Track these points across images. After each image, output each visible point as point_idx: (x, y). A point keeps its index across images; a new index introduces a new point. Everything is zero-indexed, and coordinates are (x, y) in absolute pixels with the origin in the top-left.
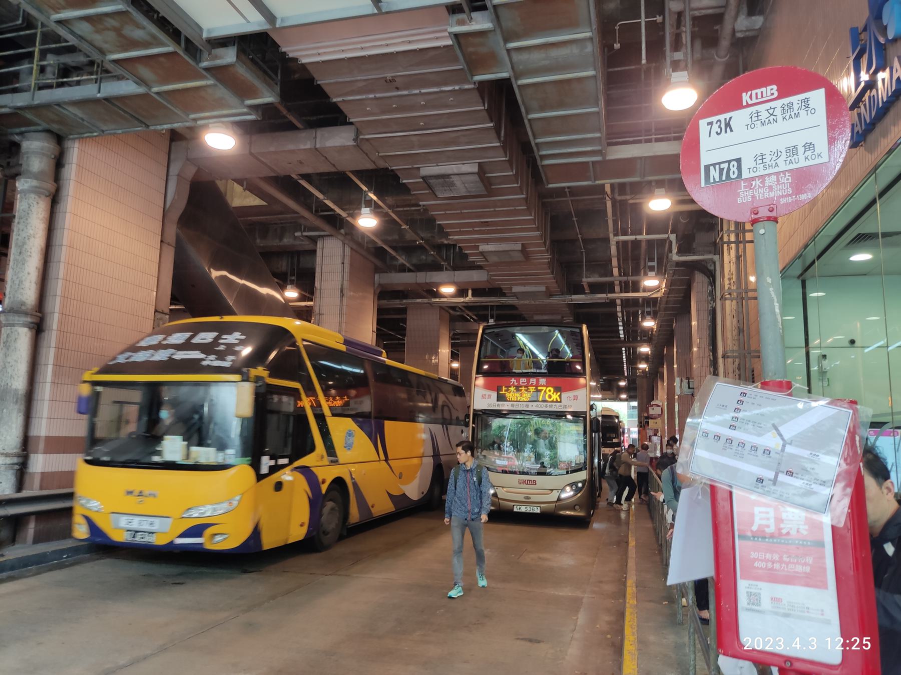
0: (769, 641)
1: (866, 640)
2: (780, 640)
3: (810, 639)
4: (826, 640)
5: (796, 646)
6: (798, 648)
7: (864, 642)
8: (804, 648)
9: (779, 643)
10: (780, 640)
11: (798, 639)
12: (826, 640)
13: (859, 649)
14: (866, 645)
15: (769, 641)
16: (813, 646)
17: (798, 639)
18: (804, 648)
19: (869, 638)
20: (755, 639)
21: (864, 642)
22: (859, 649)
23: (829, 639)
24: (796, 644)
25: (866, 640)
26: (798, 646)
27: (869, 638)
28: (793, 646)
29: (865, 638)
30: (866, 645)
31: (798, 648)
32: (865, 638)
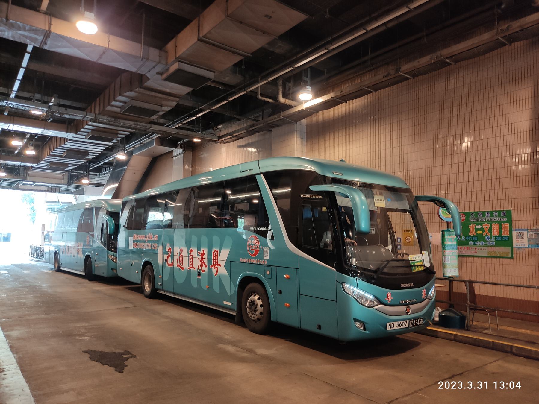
0: (454, 383)
2: (460, 383)
4: (494, 383)
5: (518, 387)
6: (519, 388)
8: (465, 388)
10: (480, 383)
11: (519, 383)
12: (494, 383)
13: (443, 388)
15: (454, 383)
16: (502, 387)
17: (519, 383)
18: (475, 388)
22: (443, 388)
23: (496, 383)
24: (518, 385)
26: (519, 387)
28: (516, 386)
31: (519, 388)
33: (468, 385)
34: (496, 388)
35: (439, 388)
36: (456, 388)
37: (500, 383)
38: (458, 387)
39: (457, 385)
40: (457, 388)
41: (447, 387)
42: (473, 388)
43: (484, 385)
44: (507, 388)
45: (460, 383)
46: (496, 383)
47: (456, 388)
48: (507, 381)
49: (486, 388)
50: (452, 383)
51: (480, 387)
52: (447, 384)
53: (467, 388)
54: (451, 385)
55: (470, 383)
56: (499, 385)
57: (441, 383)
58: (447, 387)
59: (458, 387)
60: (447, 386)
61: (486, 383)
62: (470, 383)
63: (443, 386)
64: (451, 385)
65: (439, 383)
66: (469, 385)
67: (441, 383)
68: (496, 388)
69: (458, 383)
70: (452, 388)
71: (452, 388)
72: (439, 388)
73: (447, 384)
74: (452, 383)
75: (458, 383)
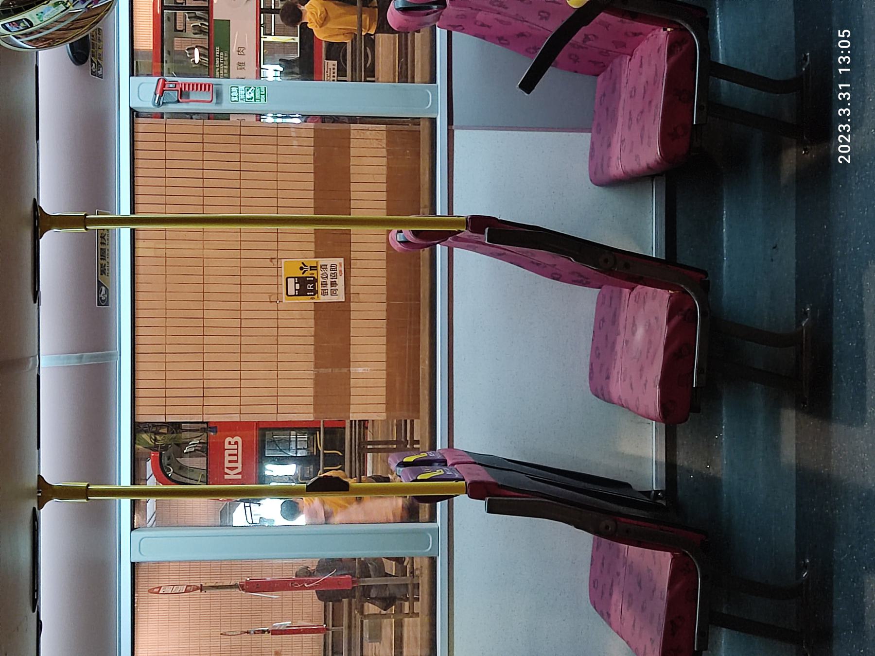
0: (842, 139)
1: (841, 34)
2: (842, 128)
3: (840, 115)
4: (841, 73)
7: (843, 36)
9: (844, 129)
10: (841, 96)
12: (841, 73)
14: (846, 34)
15: (842, 139)
16: (847, 60)
18: (849, 104)
19: (839, 31)
20: (840, 152)
21: (843, 36)
23: (840, 70)
25: (841, 34)
27: (839, 31)
29: (840, 35)
30: (846, 34)
32: (840, 35)
33: (844, 116)
34: (849, 70)
35: (849, 162)
36: (849, 135)
37: (840, 63)
38: (848, 131)
39: (845, 133)
40: (849, 133)
41: (847, 149)
42: (848, 107)
43: (844, 90)
44: (849, 52)
45: (842, 128)
46: (840, 70)
47: (849, 135)
48: (838, 52)
50: (841, 141)
51: (847, 96)
52: (842, 149)
53: (849, 117)
54: (845, 142)
55: (842, 112)
56: (844, 65)
57: (842, 159)
58: (847, 149)
59: (848, 131)
60: (846, 149)
61: (840, 86)
62: (842, 112)
63: (846, 155)
64: (845, 142)
65: (841, 162)
66: (844, 113)
67: (842, 159)
68: (849, 70)
69: (840, 131)
70: (849, 141)
71: (849, 141)
72: (849, 162)
73: (842, 149)
74: (841, 141)
75: (840, 131)
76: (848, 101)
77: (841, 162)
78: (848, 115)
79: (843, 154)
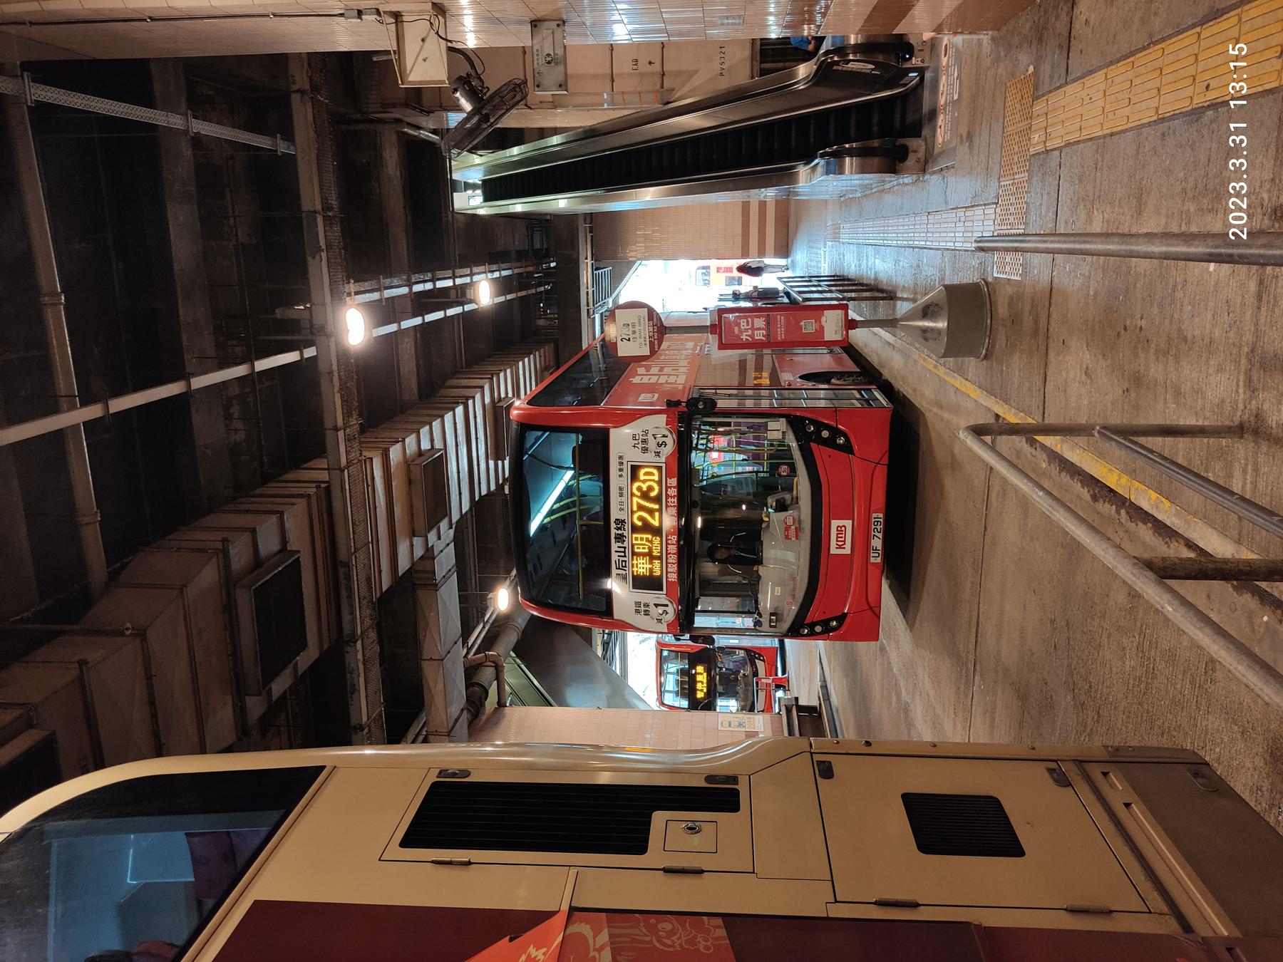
1: (1233, 49)
10: (1234, 141)
13: (1245, 229)
14: (1241, 50)
19: (1231, 46)
25: (1233, 49)
27: (1231, 46)
29: (1231, 52)
30: (1241, 50)
32: (1231, 52)
33: (1237, 170)
35: (1245, 237)
36: (1245, 198)
38: (1244, 192)
39: (1238, 195)
40: (1244, 195)
41: (1242, 218)
43: (1238, 132)
45: (1234, 188)
46: (1232, 103)
47: (1245, 198)
49: (1245, 125)
50: (1233, 207)
51: (1242, 141)
52: (1235, 218)
53: (1245, 171)
54: (1240, 209)
55: (1234, 165)
57: (1234, 234)
58: (1242, 218)
59: (1244, 192)
60: (1241, 218)
61: (1232, 126)
62: (1234, 165)
63: (1240, 228)
65: (1233, 238)
66: (1238, 166)
67: (1234, 234)
69: (1232, 192)
70: (1245, 206)
72: (1245, 237)
73: (1235, 218)
74: (1233, 207)
75: (1232, 192)
76: (1244, 149)
77: (1233, 238)
78: (1243, 169)
79: (1234, 226)
